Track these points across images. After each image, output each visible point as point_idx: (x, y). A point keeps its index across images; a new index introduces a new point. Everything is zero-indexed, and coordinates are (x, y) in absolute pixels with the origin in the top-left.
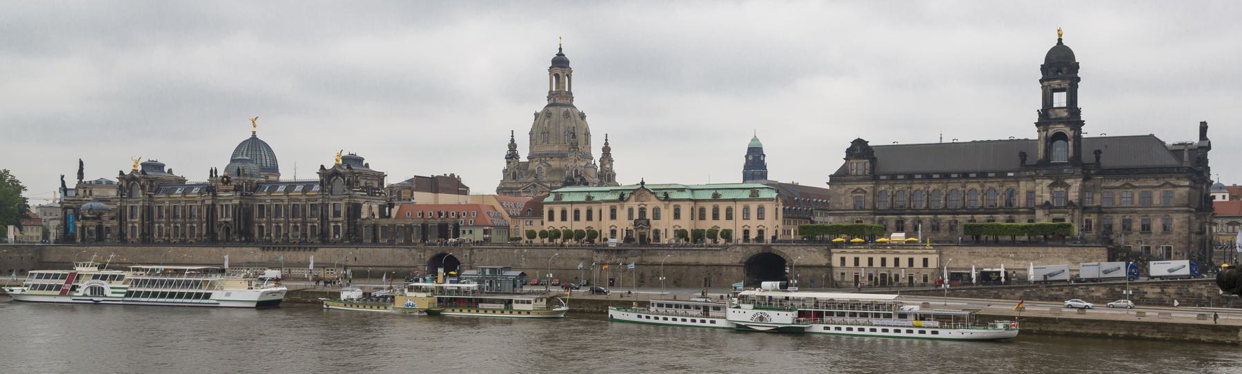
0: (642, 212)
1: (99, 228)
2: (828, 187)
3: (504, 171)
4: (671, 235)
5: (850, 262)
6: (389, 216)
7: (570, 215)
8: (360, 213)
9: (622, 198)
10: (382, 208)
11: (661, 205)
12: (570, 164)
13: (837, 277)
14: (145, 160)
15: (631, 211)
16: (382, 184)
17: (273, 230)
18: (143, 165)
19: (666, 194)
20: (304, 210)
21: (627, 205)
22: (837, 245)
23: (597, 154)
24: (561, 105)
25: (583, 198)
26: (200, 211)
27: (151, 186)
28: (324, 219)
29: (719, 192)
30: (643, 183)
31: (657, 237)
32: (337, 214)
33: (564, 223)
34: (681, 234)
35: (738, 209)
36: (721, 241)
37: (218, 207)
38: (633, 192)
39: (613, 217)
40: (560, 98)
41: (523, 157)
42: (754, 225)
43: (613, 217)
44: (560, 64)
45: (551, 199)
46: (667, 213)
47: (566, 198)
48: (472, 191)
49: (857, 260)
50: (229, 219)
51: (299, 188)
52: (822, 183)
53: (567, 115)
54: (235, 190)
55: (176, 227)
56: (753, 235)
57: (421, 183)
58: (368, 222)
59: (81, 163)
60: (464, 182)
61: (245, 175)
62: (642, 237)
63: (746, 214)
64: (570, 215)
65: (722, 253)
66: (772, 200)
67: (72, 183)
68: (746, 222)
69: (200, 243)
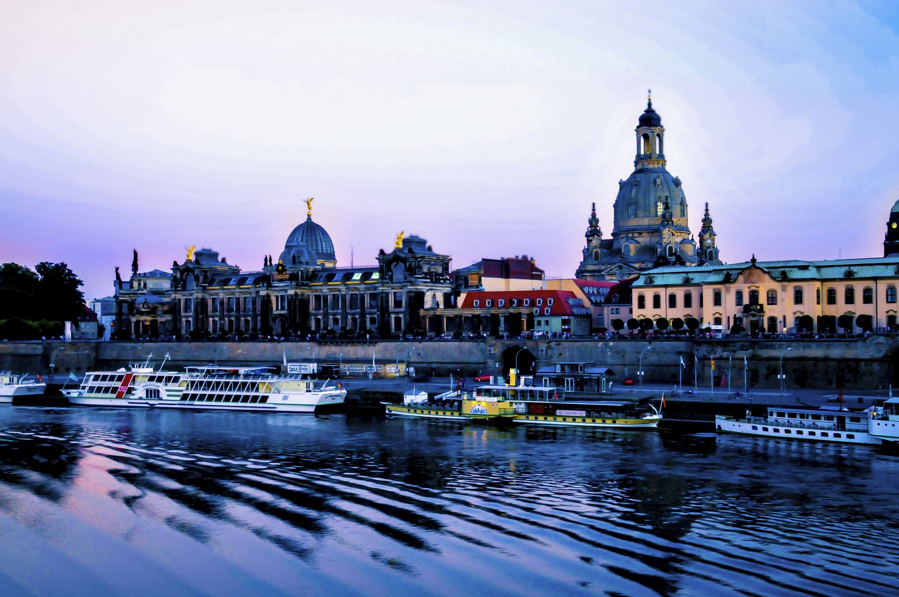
4: (791, 322)
6: (455, 306)
7: (664, 302)
10: (447, 297)
14: (198, 249)
15: (739, 294)
16: (446, 268)
18: (197, 254)
19: (784, 274)
21: (734, 288)
25: (678, 279)
26: (254, 303)
27: (206, 277)
28: (384, 310)
29: (854, 269)
30: (754, 260)
32: (398, 304)
33: (657, 311)
34: (804, 322)
35: (881, 288)
36: (858, 330)
38: (742, 271)
39: (717, 301)
41: (607, 233)
43: (717, 301)
44: (650, 121)
45: (640, 282)
47: (658, 281)
48: (548, 274)
51: (357, 276)
59: (136, 254)
60: (539, 264)
64: (664, 302)
67: (126, 276)
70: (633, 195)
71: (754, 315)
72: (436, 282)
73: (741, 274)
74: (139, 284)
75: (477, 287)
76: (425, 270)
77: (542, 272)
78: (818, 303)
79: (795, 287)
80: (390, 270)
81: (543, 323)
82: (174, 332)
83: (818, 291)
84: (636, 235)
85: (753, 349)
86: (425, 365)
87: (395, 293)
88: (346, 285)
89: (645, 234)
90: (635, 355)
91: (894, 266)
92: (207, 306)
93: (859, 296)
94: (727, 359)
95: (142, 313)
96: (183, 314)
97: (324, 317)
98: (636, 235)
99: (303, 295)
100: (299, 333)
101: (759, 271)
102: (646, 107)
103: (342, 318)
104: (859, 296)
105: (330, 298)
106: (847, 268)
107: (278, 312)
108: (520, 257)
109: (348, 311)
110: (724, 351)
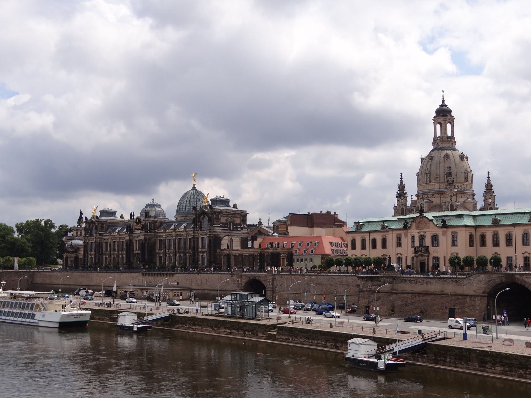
0: (422, 238)
1: (76, 258)
3: (395, 208)
7: (368, 244)
8: (220, 244)
9: (406, 227)
11: (439, 232)
14: (102, 209)
15: (413, 237)
19: (444, 221)
20: (185, 243)
23: (479, 189)
25: (379, 228)
27: (102, 227)
28: (195, 249)
31: (436, 266)
32: (203, 247)
33: (364, 252)
34: (454, 262)
37: (134, 242)
39: (399, 244)
40: (444, 143)
43: (399, 244)
44: (444, 114)
46: (445, 240)
47: (365, 229)
50: (139, 252)
53: (447, 157)
54: (142, 228)
55: (114, 257)
57: (296, 219)
58: (226, 252)
59: (81, 213)
61: (150, 217)
62: (423, 265)
64: (368, 244)
65: (465, 282)
69: (185, 269)
70: (428, 167)
71: (422, 256)
72: (233, 230)
73: (413, 221)
74: (77, 233)
75: (285, 234)
76: (223, 220)
77: (344, 223)
78: (471, 246)
79: (452, 232)
80: (199, 221)
81: (309, 260)
82: (193, 265)
83: (471, 236)
84: (430, 196)
85: (392, 283)
86: (201, 291)
87: (203, 238)
90: (329, 286)
91: (528, 215)
92: (102, 247)
93: (502, 240)
94: (374, 292)
95: (69, 252)
96: (89, 253)
98: (430, 196)
99: (150, 239)
100: (147, 267)
101: (425, 219)
102: (441, 103)
104: (502, 240)
105: (167, 241)
106: (493, 217)
107: (137, 252)
108: (324, 212)
110: (372, 285)
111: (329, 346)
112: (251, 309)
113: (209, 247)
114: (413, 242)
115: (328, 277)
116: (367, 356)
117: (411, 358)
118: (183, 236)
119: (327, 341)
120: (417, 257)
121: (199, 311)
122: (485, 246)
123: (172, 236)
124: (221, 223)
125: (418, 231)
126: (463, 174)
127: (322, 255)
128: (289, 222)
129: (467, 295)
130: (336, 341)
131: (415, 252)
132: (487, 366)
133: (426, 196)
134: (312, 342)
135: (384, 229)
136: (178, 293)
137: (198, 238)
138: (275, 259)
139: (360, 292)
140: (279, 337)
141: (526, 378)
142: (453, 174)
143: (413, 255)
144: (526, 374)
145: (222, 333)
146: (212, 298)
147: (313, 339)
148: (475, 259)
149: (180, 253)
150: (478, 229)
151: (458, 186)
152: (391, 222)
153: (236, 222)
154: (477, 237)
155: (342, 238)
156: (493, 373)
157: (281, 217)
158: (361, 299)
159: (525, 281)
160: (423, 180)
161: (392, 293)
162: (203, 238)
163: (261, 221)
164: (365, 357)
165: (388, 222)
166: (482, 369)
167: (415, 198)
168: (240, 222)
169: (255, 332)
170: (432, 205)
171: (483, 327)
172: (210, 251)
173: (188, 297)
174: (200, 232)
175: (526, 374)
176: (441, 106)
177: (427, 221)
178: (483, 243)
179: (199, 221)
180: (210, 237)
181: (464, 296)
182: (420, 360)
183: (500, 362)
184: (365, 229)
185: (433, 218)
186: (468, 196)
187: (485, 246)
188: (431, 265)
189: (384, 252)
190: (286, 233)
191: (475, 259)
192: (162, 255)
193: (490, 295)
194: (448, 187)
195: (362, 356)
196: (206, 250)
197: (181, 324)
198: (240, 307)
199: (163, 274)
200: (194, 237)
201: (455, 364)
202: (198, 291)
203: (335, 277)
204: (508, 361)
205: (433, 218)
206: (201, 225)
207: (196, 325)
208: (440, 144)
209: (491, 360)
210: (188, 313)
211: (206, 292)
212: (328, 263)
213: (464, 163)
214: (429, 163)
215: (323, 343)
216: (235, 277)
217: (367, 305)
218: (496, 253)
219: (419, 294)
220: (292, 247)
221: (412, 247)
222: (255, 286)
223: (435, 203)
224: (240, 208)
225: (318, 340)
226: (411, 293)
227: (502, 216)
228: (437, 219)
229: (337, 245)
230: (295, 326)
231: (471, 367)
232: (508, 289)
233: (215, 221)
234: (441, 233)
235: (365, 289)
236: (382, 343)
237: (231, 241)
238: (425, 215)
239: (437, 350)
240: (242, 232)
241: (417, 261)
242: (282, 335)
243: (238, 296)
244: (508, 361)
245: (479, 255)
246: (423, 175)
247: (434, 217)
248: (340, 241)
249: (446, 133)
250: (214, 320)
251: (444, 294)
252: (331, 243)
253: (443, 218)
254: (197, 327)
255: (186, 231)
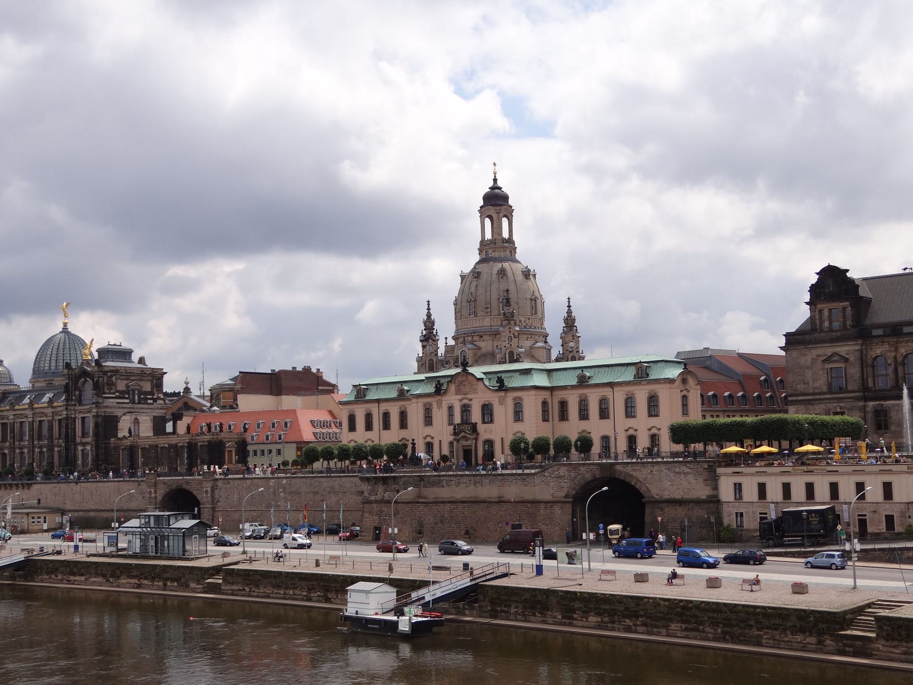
0: (466, 409)
2: (783, 353)
3: (419, 360)
5: (750, 493)
7: (377, 422)
8: (116, 429)
9: (439, 391)
11: (494, 398)
12: (503, 343)
13: (729, 520)
15: (451, 408)
17: (18, 458)
19: (500, 381)
20: (51, 428)
22: (731, 460)
23: (553, 326)
24: (496, 260)
25: (394, 394)
28: (69, 438)
31: (489, 456)
32: (84, 435)
33: (369, 435)
34: (518, 447)
39: (428, 420)
40: (497, 249)
42: (642, 425)
43: (428, 420)
44: (496, 202)
46: (503, 412)
47: (371, 396)
49: (762, 488)
52: (770, 344)
53: (502, 273)
56: (643, 443)
57: (250, 382)
58: (127, 442)
63: (630, 411)
64: (377, 422)
65: (537, 480)
66: (671, 381)
68: (631, 422)
69: (49, 475)
73: (450, 381)
75: (232, 407)
77: (334, 386)
78: (544, 420)
82: (63, 466)
83: (545, 403)
84: (476, 338)
86: (81, 514)
87: (83, 419)
88: (33, 409)
89: (485, 337)
90: (311, 496)
91: (633, 368)
94: (389, 502)
97: (10, 451)
98: (476, 338)
101: (470, 378)
102: (491, 184)
103: (29, 452)
105: (17, 426)
106: (579, 371)
109: (36, 442)
111: (314, 599)
112: (176, 542)
113: (96, 434)
114: (451, 415)
115: (308, 480)
116: (380, 612)
117: (453, 611)
118: (46, 416)
119: (310, 590)
120: (458, 441)
121: (80, 549)
122: (567, 420)
123: (27, 417)
124: (118, 391)
125: (460, 397)
126: (528, 302)
127: (297, 443)
128: (239, 386)
129: (540, 502)
130: (327, 589)
131: (455, 434)
132: (575, 616)
133: (470, 339)
134: (285, 594)
135: (402, 395)
136: (39, 518)
137: (75, 418)
138: (215, 452)
139: (364, 503)
140: (228, 587)
141: (636, 632)
142: (512, 301)
143: (452, 438)
144: (636, 625)
145: (124, 586)
146: (105, 525)
147: (286, 588)
148: (551, 443)
149: (41, 447)
150: (555, 393)
151: (520, 321)
152: (415, 384)
153: (144, 390)
154: (555, 406)
155: (331, 412)
156: (585, 628)
157: (224, 377)
158: (366, 515)
159: (630, 476)
160: (465, 312)
161: (418, 502)
162: (83, 419)
163: (189, 386)
164: (377, 614)
165: (409, 384)
166: (567, 621)
167: (451, 342)
168: (152, 388)
169: (183, 580)
170: (479, 353)
171: (567, 554)
172: (97, 441)
173: (58, 526)
174: (78, 408)
175: (636, 625)
176: (492, 188)
177: (475, 381)
178: (564, 416)
179: (76, 389)
180: (96, 416)
181: (535, 502)
182: (467, 612)
183: (596, 609)
184: (371, 396)
185: (483, 376)
186: (537, 338)
187: (567, 420)
188: (480, 453)
189: (404, 434)
190: (233, 406)
191: (551, 443)
192: (6, 451)
193: (577, 499)
194: (505, 323)
195: (373, 612)
196: (89, 440)
197: (47, 574)
198: (156, 538)
199: (11, 485)
200: (67, 418)
201: (524, 615)
202: (76, 514)
203: (322, 480)
204: (607, 607)
205: (483, 376)
206: (80, 395)
207: (74, 574)
208: (490, 251)
209: (581, 606)
210: (59, 553)
211: (92, 514)
212: (309, 455)
213: (529, 283)
214: (474, 284)
215: (305, 593)
216: (144, 486)
217: (376, 525)
218: (584, 431)
219: (463, 502)
220: (246, 430)
221: (450, 424)
222: (182, 501)
223: (484, 350)
224: (151, 364)
225: (296, 588)
226: (450, 502)
227: (593, 370)
228: (490, 376)
229: (324, 424)
230: (255, 566)
231: (550, 620)
232: (605, 488)
233: (106, 387)
234: (497, 400)
235: (373, 498)
236: (405, 588)
237: (136, 422)
238: (471, 370)
239: (494, 596)
240: (155, 405)
241: (458, 449)
242: (233, 584)
243: (152, 519)
244: (607, 607)
245: (558, 434)
246: (464, 304)
247: (484, 373)
248: (328, 418)
249: (501, 234)
250: (109, 564)
251: (505, 502)
252: (312, 422)
253: (499, 375)
254: (77, 578)
255: (53, 407)
